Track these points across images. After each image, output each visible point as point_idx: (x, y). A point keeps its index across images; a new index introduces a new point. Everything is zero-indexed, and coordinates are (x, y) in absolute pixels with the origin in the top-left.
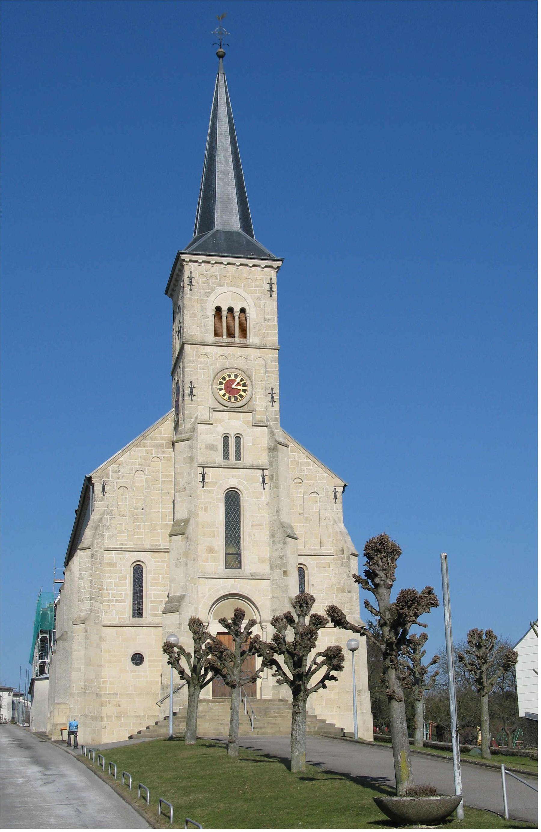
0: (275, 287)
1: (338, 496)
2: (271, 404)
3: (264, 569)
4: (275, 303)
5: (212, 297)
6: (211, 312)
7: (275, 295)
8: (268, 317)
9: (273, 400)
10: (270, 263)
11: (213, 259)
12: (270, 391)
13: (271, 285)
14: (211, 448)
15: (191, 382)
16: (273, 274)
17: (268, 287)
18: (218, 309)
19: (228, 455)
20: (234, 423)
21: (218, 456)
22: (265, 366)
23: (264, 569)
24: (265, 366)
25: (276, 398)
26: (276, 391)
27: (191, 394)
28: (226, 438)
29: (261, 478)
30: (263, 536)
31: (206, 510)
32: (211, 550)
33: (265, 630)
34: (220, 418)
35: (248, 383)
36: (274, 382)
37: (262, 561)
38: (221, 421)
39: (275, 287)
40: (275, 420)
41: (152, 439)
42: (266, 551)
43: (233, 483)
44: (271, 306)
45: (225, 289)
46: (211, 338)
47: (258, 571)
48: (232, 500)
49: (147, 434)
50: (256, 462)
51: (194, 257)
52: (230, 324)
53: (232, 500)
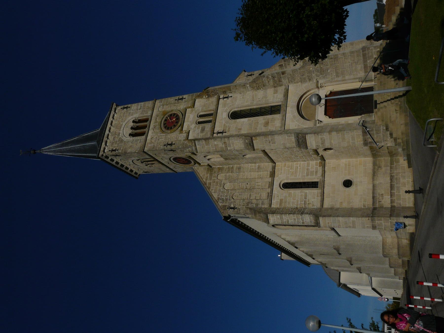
0: (125, 106)
1: (250, 74)
2: (184, 100)
3: (281, 90)
4: (133, 105)
5: (124, 138)
6: (132, 138)
7: (129, 105)
8: (139, 107)
9: (182, 99)
10: (113, 109)
11: (105, 139)
12: (177, 101)
13: (124, 108)
14: (203, 130)
15: (165, 145)
16: (119, 108)
17: (125, 110)
18: (130, 135)
19: (210, 121)
20: (190, 119)
21: (208, 127)
22: (163, 105)
23: (281, 90)
24: (163, 105)
25: (181, 97)
26: (177, 98)
27: (171, 145)
28: (200, 123)
29: (225, 99)
30: (260, 93)
31: (240, 129)
32: (267, 124)
33: (324, 85)
34: (186, 127)
35: (170, 113)
36: (172, 100)
37: (276, 92)
38: (188, 126)
39: (125, 106)
40: (192, 96)
41: (207, 180)
42: (270, 91)
43: (225, 115)
44: (134, 106)
45: (121, 132)
46: (144, 137)
47: (283, 93)
48: (235, 115)
49: (203, 183)
50: (215, 103)
51: (102, 149)
52: (140, 128)
53: (235, 115)
